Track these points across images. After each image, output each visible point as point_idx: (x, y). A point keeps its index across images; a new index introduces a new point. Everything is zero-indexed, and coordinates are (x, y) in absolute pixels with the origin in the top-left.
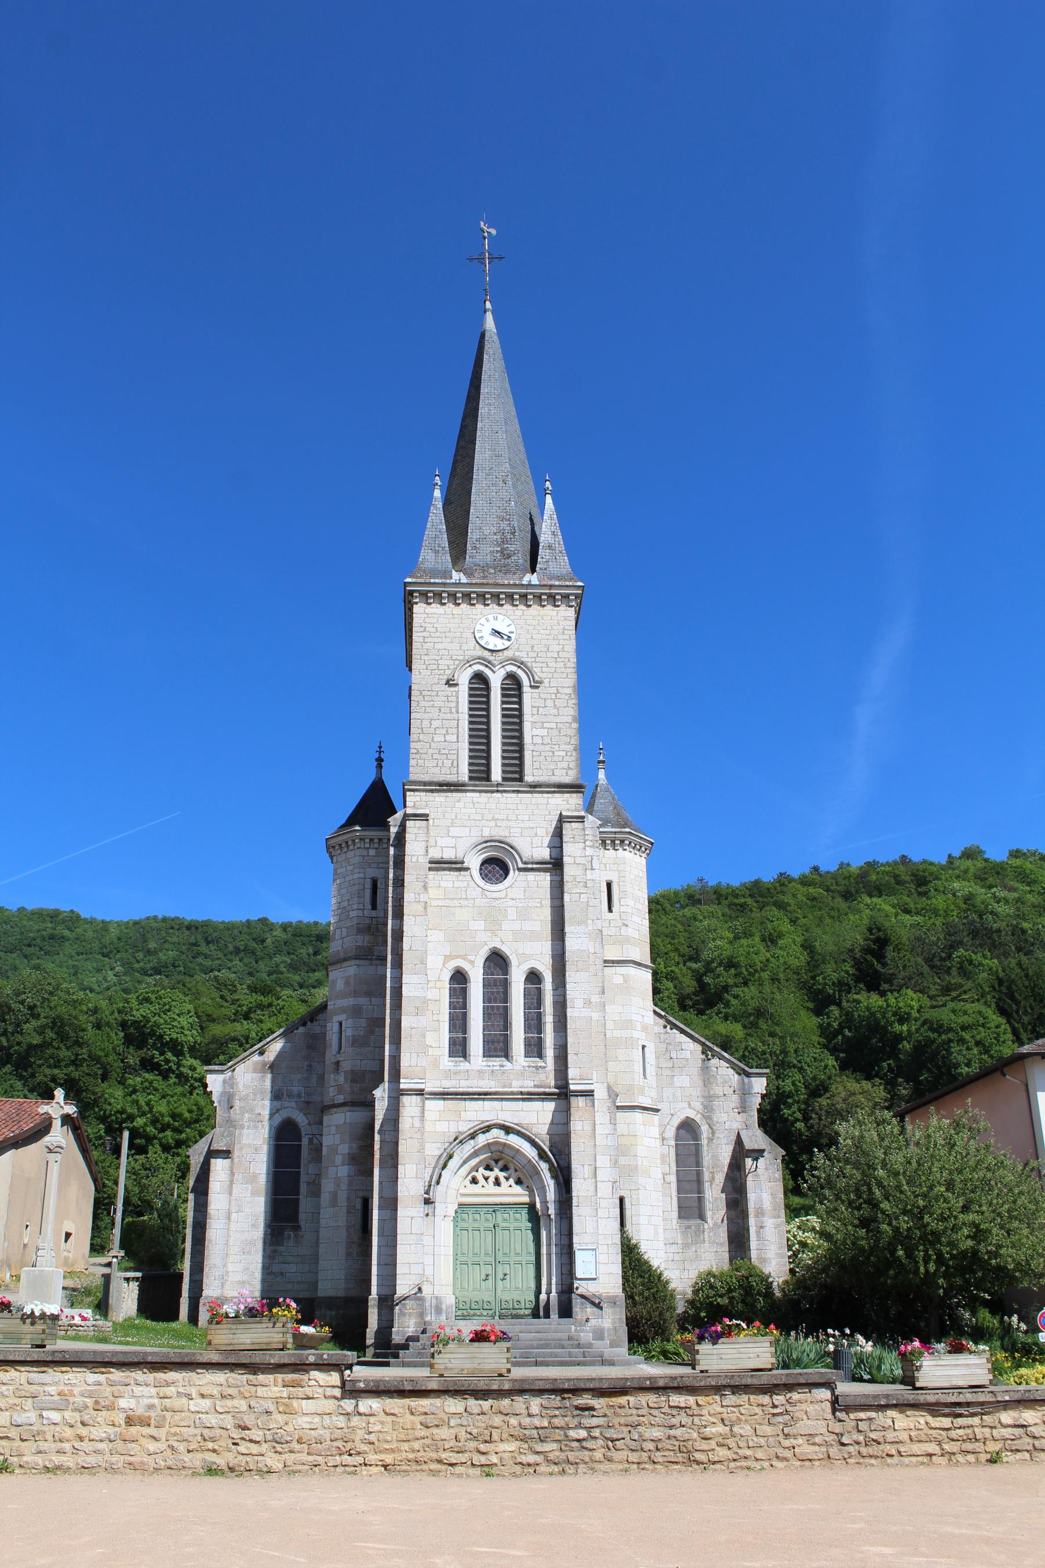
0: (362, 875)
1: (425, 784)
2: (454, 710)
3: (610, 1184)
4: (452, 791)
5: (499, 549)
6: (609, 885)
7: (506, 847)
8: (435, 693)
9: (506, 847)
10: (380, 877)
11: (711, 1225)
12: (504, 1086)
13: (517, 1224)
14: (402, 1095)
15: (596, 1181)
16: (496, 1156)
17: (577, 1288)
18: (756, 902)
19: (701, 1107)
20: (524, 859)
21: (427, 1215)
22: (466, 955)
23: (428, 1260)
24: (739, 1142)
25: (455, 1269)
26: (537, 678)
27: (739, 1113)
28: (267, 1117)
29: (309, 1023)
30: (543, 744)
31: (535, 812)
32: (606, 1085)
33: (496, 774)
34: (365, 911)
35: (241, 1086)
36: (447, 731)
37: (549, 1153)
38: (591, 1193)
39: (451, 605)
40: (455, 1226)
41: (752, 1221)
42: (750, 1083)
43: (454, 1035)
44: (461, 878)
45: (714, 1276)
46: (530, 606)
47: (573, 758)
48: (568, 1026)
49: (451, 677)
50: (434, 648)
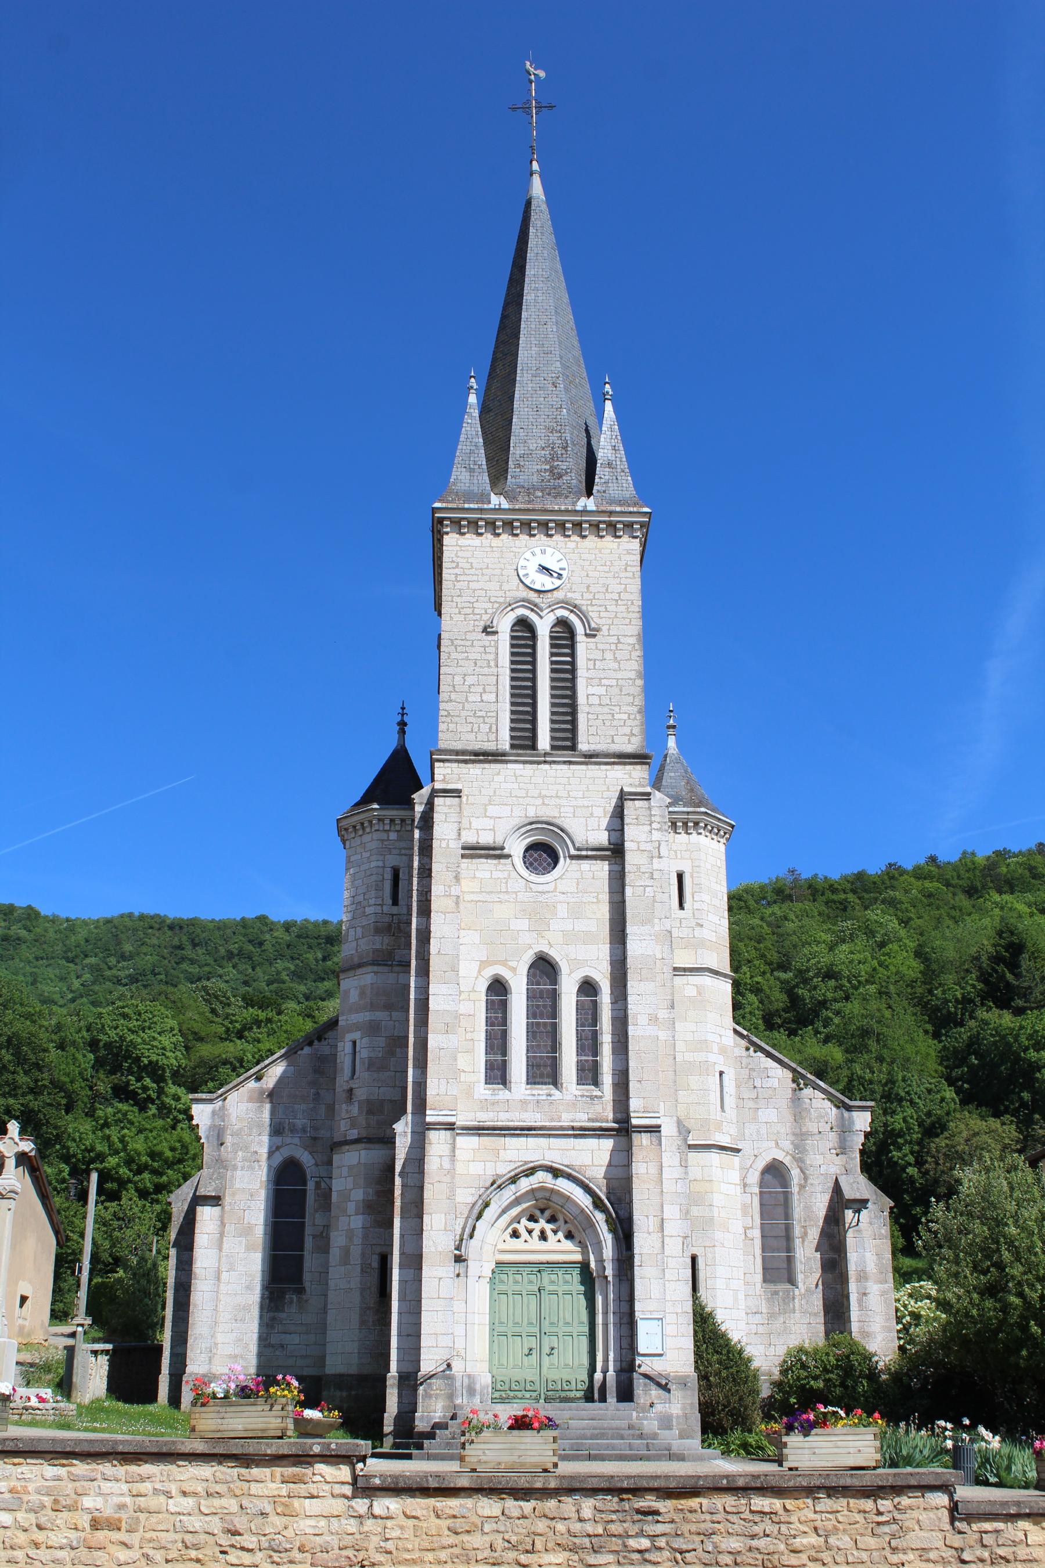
0: (380, 864)
1: (457, 753)
2: (492, 663)
3: (680, 1240)
4: (490, 762)
5: (548, 467)
6: (680, 877)
7: (556, 829)
8: (469, 643)
9: (556, 829)
10: (402, 865)
11: (803, 1291)
12: (552, 1120)
13: (566, 1288)
14: (429, 1129)
15: (663, 1236)
17: (640, 1366)
18: (860, 898)
19: (791, 1147)
20: (577, 845)
21: (458, 1275)
22: (506, 960)
23: (460, 1330)
24: (837, 1189)
25: (492, 1342)
26: (593, 625)
27: (837, 1155)
28: (265, 1156)
29: (316, 1042)
30: (600, 705)
32: (675, 1118)
33: (544, 741)
34: (385, 908)
36: (484, 689)
37: (606, 1201)
39: (489, 536)
40: (492, 1289)
41: (853, 1287)
42: (851, 1118)
43: (492, 1057)
44: (500, 867)
45: (807, 1353)
46: (585, 537)
47: (637, 722)
48: (630, 1048)
49: (488, 623)
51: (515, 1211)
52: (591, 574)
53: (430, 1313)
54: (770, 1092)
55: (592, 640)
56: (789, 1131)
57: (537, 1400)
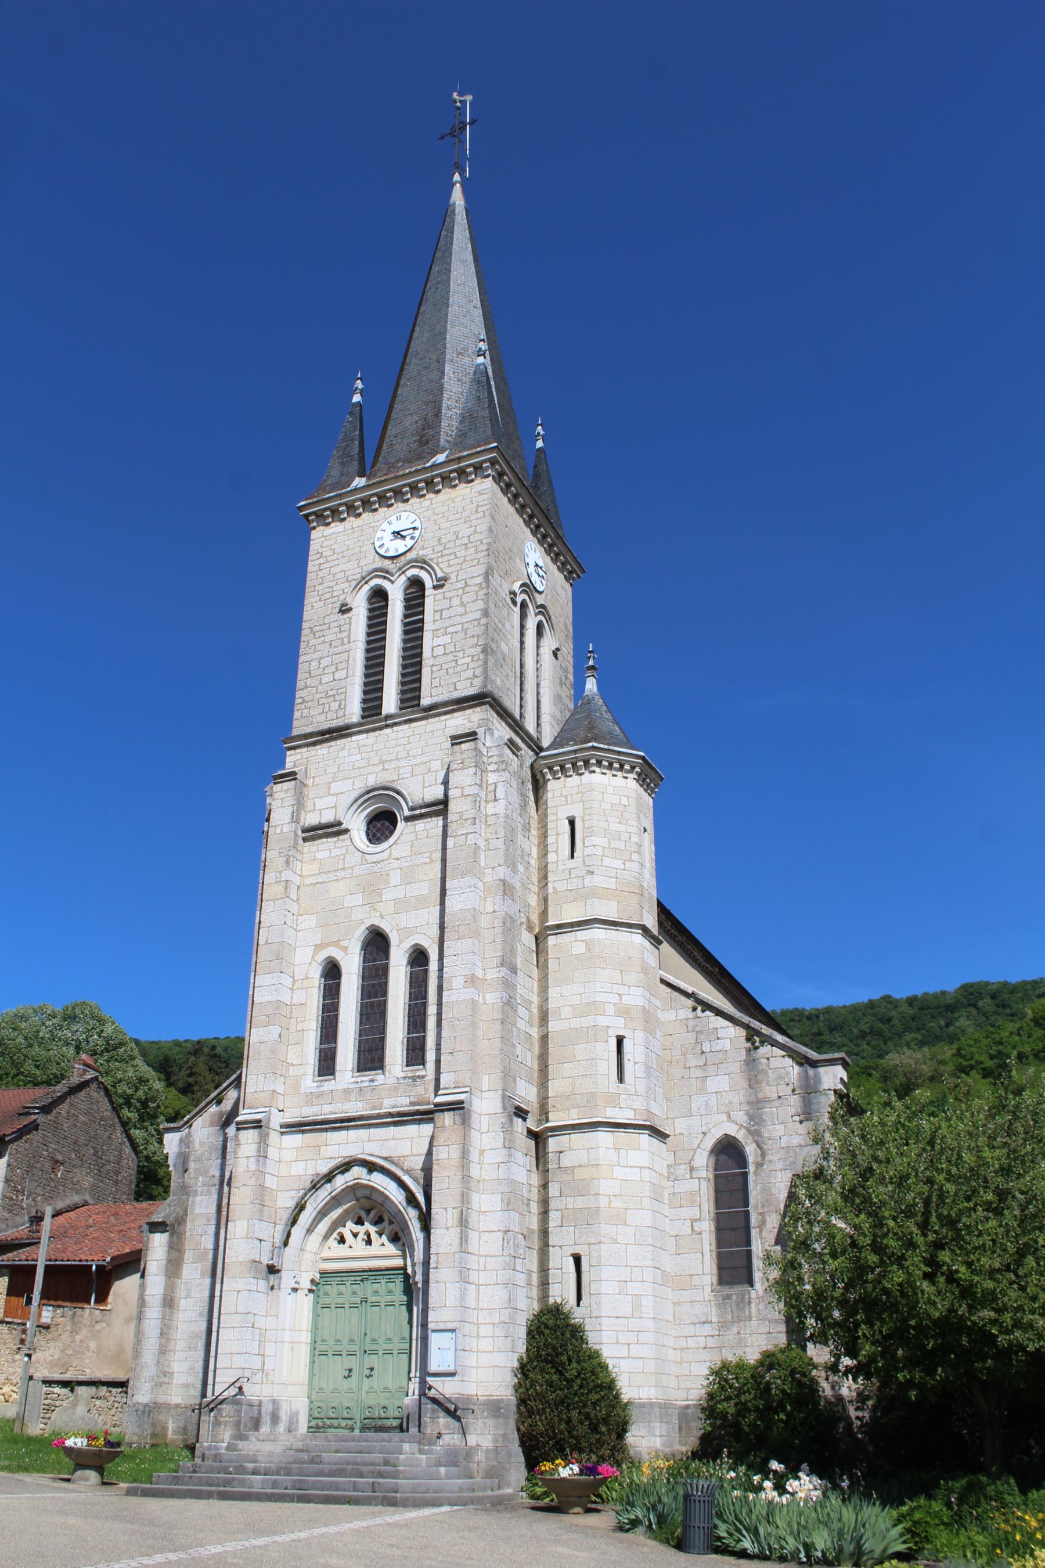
2: (346, 641)
3: (500, 1235)
6: (572, 823)
11: (761, 1292)
12: (374, 1108)
13: (389, 1298)
16: (367, 1204)
19: (746, 1118)
21: (272, 1288)
22: (339, 940)
25: (313, 1362)
27: (801, 1122)
30: (445, 654)
31: (430, 742)
33: (390, 703)
35: (197, 1145)
36: (337, 668)
38: (455, 1248)
40: (316, 1303)
43: (323, 1046)
44: (340, 844)
46: (439, 491)
50: (330, 574)
51: (335, 1214)
52: (442, 526)
53: (227, 1330)
54: (721, 1056)
56: (743, 1099)
57: (352, 1429)
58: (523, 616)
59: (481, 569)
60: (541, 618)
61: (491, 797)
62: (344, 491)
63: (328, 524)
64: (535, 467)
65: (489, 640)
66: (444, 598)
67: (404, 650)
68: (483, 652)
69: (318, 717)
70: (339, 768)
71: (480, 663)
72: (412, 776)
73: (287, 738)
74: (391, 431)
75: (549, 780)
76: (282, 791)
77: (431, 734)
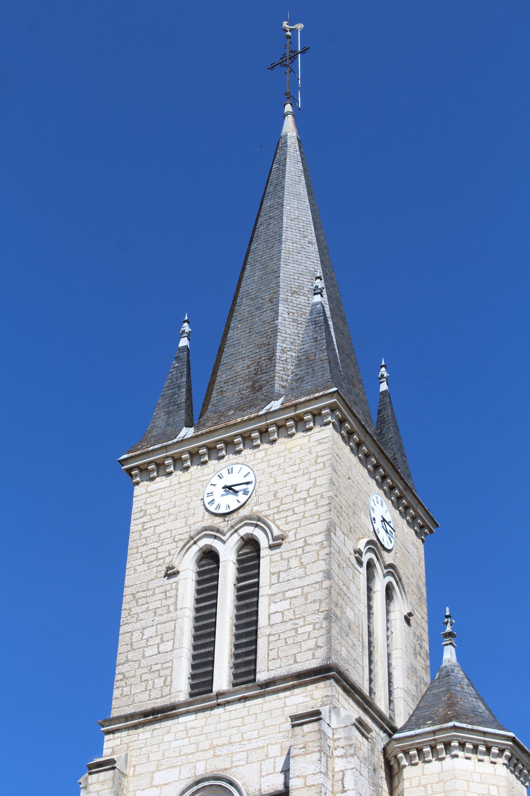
1: (126, 718)
2: (172, 608)
4: (160, 720)
30: (283, 622)
31: (267, 723)
36: (162, 639)
52: (279, 479)
55: (277, 551)
58: (370, 578)
59: (322, 526)
60: (390, 579)
61: (338, 787)
62: (170, 442)
63: (153, 479)
64: (379, 412)
65: (333, 606)
66: (282, 559)
67: (238, 617)
68: (326, 619)
69: (140, 695)
70: (163, 755)
71: (323, 631)
72: (247, 763)
73: (105, 721)
74: (222, 376)
75: (405, 766)
76: (98, 782)
77: (268, 714)
